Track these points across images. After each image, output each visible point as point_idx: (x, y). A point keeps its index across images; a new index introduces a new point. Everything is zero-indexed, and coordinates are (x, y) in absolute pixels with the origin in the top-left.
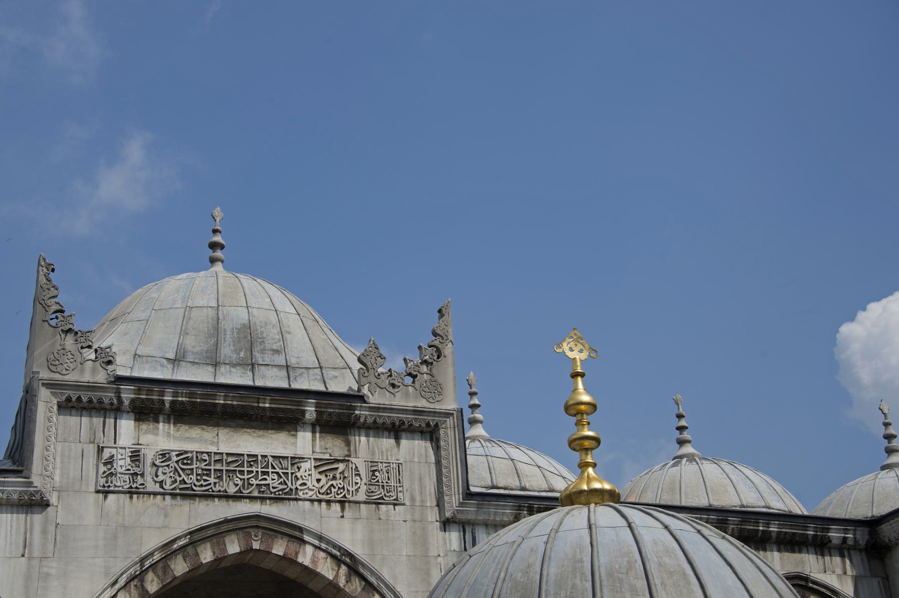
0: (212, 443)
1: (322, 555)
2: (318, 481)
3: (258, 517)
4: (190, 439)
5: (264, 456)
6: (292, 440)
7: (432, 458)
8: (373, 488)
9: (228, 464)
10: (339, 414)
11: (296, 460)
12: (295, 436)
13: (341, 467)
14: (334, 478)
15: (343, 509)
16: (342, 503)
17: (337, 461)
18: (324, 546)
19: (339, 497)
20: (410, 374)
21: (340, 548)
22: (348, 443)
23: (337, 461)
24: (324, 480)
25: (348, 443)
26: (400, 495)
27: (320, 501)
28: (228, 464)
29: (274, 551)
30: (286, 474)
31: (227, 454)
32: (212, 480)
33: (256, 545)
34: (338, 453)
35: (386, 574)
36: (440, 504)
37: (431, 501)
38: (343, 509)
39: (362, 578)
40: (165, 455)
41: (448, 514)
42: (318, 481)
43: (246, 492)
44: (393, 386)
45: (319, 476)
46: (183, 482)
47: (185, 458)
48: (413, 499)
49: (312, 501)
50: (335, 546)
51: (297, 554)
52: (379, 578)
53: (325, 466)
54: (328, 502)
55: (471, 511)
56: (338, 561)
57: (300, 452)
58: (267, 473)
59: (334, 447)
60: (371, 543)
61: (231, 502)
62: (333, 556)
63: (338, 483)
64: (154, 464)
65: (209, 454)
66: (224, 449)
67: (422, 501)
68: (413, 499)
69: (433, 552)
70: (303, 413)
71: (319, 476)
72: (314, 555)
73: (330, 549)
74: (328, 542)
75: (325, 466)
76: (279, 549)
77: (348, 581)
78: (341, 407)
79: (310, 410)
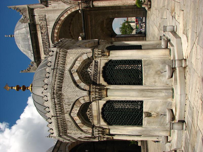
0: (42, 47)
3: (51, 39)
4: (42, 50)
5: (42, 39)
8: (44, 20)
9: (44, 44)
11: (42, 33)
13: (41, 26)
14: (43, 27)
15: (48, 25)
16: (47, 25)
19: (46, 26)
20: (23, 14)
22: (37, 24)
24: (43, 29)
27: (47, 29)
28: (44, 44)
29: (56, 36)
32: (47, 47)
33: (56, 39)
35: (57, 17)
36: (43, 8)
38: (48, 25)
39: (58, 21)
40: (45, 54)
43: (48, 41)
44: (26, 17)
46: (48, 51)
47: (45, 51)
48: (44, 13)
51: (56, 32)
54: (47, 28)
57: (40, 33)
58: (45, 38)
60: (52, 20)
61: (50, 43)
64: (46, 55)
65: (43, 47)
67: (44, 11)
68: (44, 13)
69: (52, 9)
74: (53, 27)
76: (56, 35)
78: (31, 26)
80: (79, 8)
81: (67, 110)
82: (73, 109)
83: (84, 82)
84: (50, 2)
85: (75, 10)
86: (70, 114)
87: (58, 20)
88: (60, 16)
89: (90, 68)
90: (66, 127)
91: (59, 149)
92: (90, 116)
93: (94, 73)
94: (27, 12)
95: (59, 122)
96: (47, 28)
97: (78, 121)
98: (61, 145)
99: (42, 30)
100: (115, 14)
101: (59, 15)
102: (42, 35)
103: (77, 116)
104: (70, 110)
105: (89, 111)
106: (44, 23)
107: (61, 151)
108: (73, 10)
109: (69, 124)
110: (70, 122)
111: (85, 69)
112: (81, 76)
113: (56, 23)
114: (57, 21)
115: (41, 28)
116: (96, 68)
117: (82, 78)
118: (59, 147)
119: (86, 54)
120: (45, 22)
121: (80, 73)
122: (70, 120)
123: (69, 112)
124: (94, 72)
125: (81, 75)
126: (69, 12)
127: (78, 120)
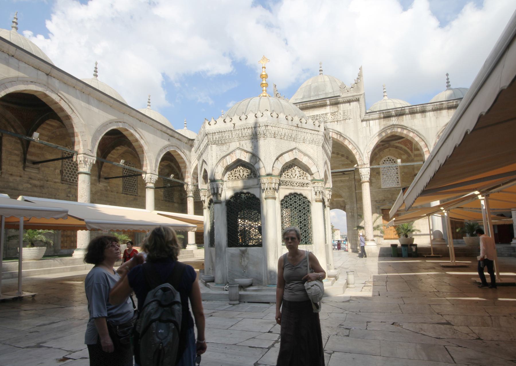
1: (334, 133)
2: (332, 117)
5: (319, 115)
6: (325, 110)
7: (359, 107)
10: (335, 101)
11: (326, 114)
12: (326, 109)
13: (337, 113)
14: (335, 116)
15: (337, 122)
17: (335, 112)
18: (334, 131)
19: (336, 120)
21: (337, 131)
23: (335, 112)
24: (333, 117)
25: (338, 108)
26: (351, 117)
27: (332, 122)
28: (312, 118)
30: (324, 117)
31: (312, 116)
34: (336, 111)
35: (348, 135)
36: (360, 116)
37: (358, 117)
38: (337, 122)
41: (362, 119)
42: (332, 117)
45: (331, 116)
49: (330, 122)
50: (336, 131)
52: (346, 136)
53: (333, 114)
55: (367, 117)
56: (337, 134)
57: (327, 112)
58: (320, 118)
59: (334, 109)
62: (336, 133)
63: (336, 117)
66: (311, 115)
68: (354, 117)
70: (327, 103)
71: (331, 116)
72: (332, 134)
73: (335, 131)
74: (335, 130)
75: (333, 114)
77: (340, 137)
79: (328, 102)
80: (360, 164)
81: (244, 145)
82: (246, 153)
83: (374, 152)
84: (368, 125)
85: (357, 160)
86: (239, 148)
87: (345, 137)
88: (349, 140)
89: (300, 176)
90: (220, 143)
91: (171, 136)
92: (238, 177)
93: (294, 182)
94: (355, 94)
95: (227, 134)
96: (334, 122)
97: (230, 160)
98: (177, 140)
99: (331, 114)
100: (351, 212)
101: (351, 138)
102: (325, 115)
103: (237, 158)
104: (246, 149)
105: (244, 175)
106: (340, 117)
107: (169, 140)
108: (357, 157)
109: (224, 148)
110: (228, 149)
111: (298, 170)
112: (290, 164)
113: (339, 133)
114: (343, 135)
115: (333, 113)
116: (300, 185)
117: (287, 166)
118: (174, 137)
119: (317, 171)
120: (341, 119)
121: (293, 163)
122: (231, 149)
123: (241, 147)
124: (296, 182)
125: (290, 165)
126: (354, 152)
127: (232, 160)
